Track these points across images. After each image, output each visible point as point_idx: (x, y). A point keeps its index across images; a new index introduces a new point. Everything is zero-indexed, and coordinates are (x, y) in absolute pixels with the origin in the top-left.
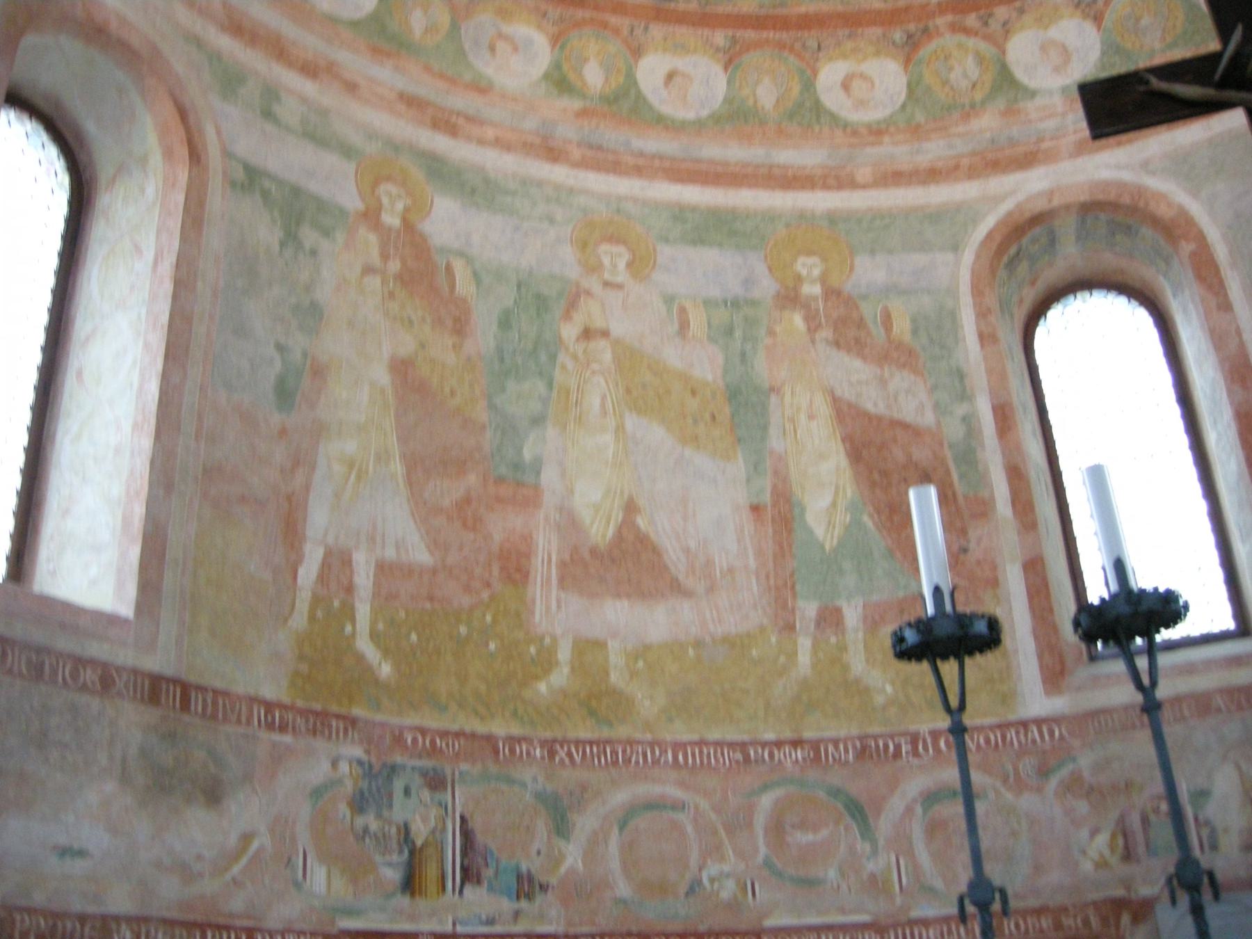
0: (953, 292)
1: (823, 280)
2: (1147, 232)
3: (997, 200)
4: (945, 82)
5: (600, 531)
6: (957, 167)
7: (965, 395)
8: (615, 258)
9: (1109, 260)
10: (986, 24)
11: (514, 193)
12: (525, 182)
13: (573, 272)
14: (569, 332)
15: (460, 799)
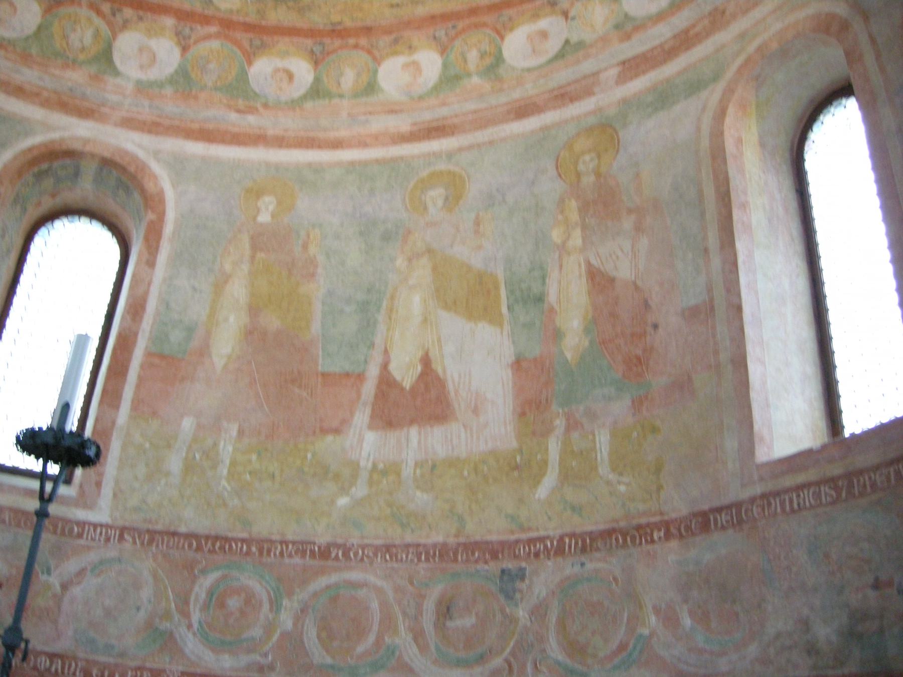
2: (136, 196)
3: (48, 127)
4: (65, 37)
6: (37, 95)
9: (111, 205)
10: (114, 15)
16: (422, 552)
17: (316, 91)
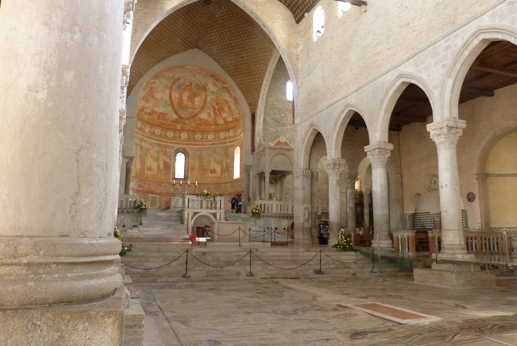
5: (149, 167)
7: (171, 161)
8: (152, 147)
15: (141, 182)
16: (215, 184)
17: (202, 138)
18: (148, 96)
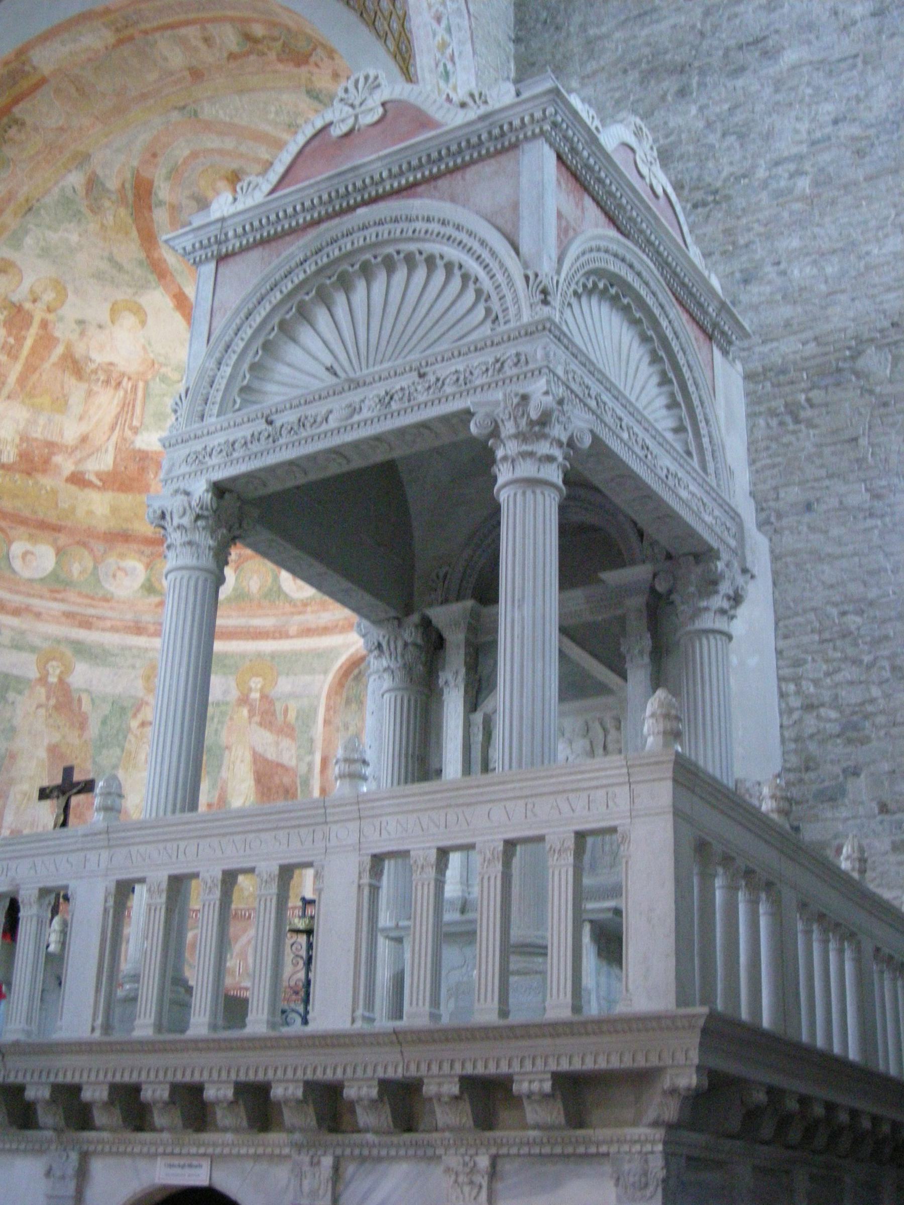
0: (318, 697)
1: (262, 690)
6: (336, 626)
7: (311, 752)
11: (116, 655)
12: (124, 648)
13: (141, 693)
14: (134, 724)
18: (30, 368)
